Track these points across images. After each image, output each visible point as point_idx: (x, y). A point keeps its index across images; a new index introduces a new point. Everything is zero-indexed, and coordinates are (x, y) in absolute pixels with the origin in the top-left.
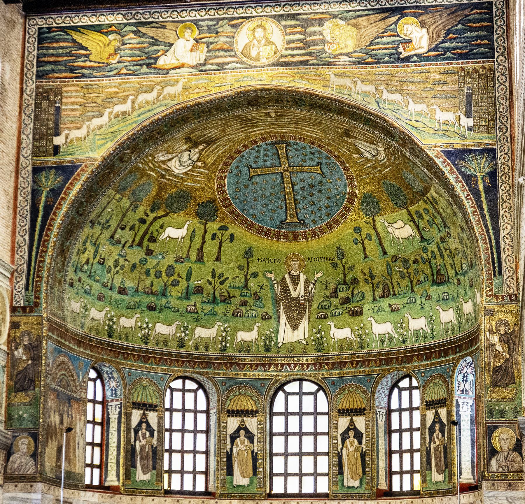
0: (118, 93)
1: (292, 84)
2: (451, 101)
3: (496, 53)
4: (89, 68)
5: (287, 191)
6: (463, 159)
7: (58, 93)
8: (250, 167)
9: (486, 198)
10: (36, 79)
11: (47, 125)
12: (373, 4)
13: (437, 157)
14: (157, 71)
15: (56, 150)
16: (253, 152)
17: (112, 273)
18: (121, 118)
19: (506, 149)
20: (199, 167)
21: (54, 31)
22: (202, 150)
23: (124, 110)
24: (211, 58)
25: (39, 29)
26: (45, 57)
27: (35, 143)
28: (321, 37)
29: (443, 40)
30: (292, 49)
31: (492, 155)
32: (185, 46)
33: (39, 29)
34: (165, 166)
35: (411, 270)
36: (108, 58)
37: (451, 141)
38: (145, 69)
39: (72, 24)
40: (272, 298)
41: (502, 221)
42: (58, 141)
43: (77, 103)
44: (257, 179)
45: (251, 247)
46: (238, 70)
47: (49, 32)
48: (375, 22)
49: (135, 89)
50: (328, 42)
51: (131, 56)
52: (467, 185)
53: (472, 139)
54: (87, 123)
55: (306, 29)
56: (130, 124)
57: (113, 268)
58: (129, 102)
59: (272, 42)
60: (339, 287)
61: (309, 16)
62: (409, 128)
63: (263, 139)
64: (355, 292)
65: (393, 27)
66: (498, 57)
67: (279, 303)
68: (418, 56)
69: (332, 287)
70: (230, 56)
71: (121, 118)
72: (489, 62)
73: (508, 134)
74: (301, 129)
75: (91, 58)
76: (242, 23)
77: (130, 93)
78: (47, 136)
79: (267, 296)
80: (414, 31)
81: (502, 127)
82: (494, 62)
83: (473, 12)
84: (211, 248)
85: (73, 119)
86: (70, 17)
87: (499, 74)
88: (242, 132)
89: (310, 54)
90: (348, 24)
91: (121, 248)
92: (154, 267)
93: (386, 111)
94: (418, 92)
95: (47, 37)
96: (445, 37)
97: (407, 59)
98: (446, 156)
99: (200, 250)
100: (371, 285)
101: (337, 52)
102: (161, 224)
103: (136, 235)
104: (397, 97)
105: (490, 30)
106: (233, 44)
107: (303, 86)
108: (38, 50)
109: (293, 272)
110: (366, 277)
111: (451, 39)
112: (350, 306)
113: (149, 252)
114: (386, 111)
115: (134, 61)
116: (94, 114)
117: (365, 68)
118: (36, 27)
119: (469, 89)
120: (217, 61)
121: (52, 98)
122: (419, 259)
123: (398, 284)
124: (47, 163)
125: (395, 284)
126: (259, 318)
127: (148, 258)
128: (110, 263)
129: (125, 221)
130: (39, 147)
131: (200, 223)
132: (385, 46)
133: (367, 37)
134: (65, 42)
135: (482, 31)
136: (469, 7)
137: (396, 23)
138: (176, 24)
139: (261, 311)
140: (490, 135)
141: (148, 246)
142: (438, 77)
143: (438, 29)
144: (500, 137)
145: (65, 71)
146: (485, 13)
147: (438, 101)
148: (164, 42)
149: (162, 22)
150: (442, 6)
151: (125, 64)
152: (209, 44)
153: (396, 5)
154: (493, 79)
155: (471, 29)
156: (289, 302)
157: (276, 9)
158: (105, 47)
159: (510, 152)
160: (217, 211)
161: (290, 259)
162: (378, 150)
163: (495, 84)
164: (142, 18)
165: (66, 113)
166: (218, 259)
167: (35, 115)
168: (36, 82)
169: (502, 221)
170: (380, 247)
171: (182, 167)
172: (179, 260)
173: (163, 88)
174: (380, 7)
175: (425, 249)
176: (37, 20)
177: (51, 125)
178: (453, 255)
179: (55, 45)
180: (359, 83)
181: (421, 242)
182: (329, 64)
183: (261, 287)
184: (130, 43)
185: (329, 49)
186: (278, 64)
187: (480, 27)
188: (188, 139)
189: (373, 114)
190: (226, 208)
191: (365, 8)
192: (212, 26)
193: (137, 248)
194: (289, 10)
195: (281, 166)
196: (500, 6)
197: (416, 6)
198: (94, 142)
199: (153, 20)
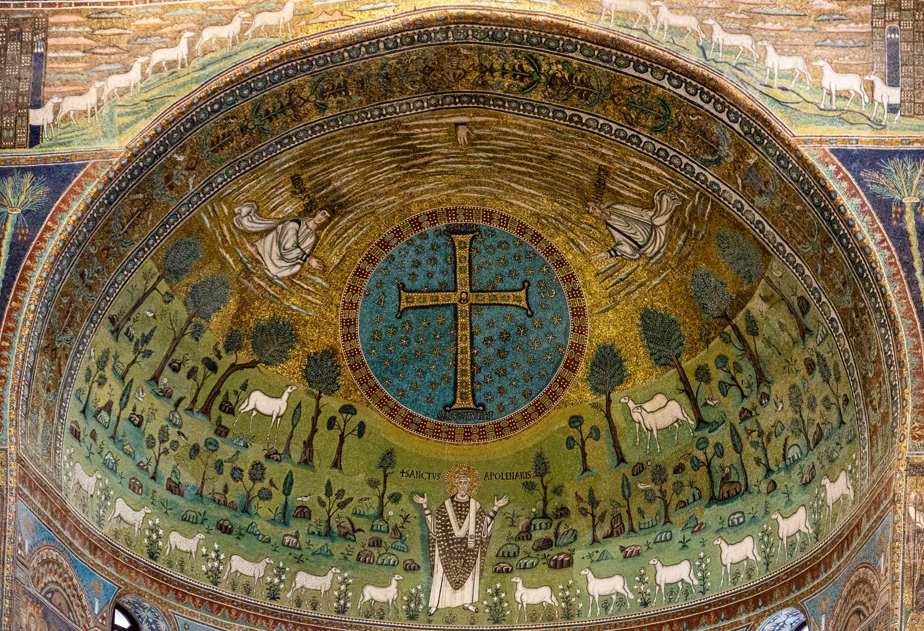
5: (461, 345)
8: (402, 287)
22: (321, 227)
23: (175, 58)
35: (668, 486)
40: (422, 537)
44: (411, 316)
45: (392, 450)
60: (534, 522)
62: (766, 103)
63: (433, 217)
64: (562, 530)
67: (434, 547)
69: (522, 522)
71: (166, 73)
79: (413, 533)
100: (590, 517)
110: (582, 505)
112: (553, 553)
123: (641, 512)
125: (634, 512)
126: (400, 567)
139: (403, 557)
156: (449, 545)
160: (339, 374)
162: (653, 227)
181: (698, 429)
183: (405, 519)
190: (353, 369)
195: (455, 290)
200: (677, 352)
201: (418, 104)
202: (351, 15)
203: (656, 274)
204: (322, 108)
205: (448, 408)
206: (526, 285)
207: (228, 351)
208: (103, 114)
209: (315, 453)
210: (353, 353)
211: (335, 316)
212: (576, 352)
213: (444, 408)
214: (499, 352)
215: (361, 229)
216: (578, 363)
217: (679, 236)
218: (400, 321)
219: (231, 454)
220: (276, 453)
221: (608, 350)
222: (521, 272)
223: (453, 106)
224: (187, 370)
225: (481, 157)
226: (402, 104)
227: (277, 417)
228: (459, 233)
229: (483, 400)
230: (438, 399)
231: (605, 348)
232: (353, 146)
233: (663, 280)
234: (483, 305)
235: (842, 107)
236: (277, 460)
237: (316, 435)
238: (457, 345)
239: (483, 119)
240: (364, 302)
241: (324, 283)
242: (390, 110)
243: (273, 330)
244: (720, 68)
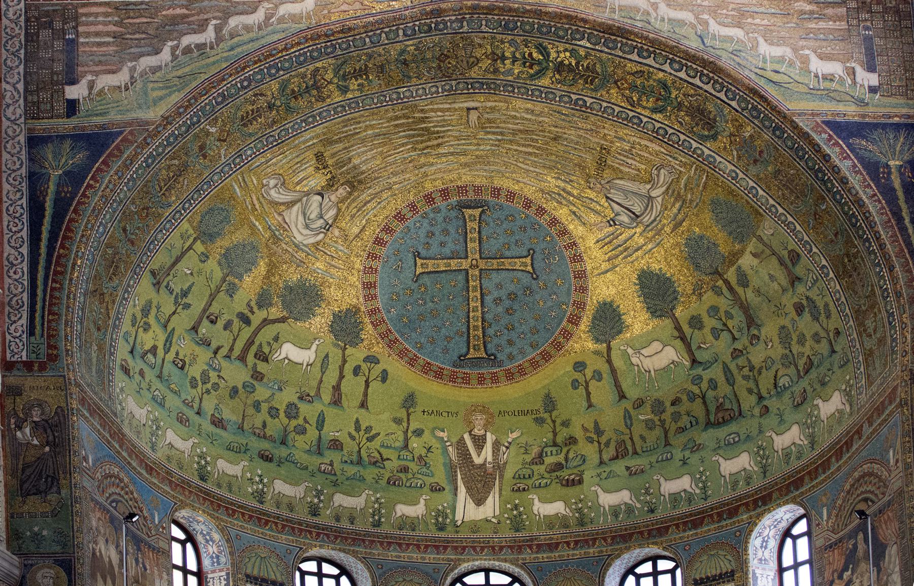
18: (196, 54)
27: (30, 98)
37: (841, 108)
42: (73, 92)
102: (275, 334)
109: (476, 430)
201: (434, 89)
204: (344, 90)
206: (531, 253)
207: (260, 307)
219: (267, 396)
220: (308, 395)
222: (527, 242)
223: (465, 91)
224: (224, 322)
225: (490, 139)
226: (419, 89)
228: (469, 207)
235: (828, 87)
236: (309, 401)
237: (344, 380)
239: (493, 104)
242: (407, 94)
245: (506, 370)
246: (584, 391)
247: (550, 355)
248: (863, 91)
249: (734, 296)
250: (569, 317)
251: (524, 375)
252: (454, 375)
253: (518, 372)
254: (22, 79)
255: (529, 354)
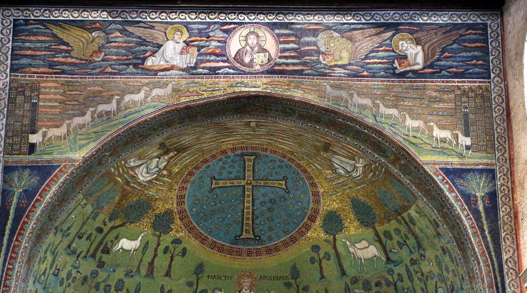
0: (101, 92)
1: (289, 93)
2: (448, 119)
3: (492, 74)
4: (71, 64)
5: (246, 205)
6: (462, 178)
7: (35, 88)
9: (486, 219)
10: (10, 73)
11: (22, 122)
12: (368, 18)
13: (435, 174)
14: (144, 72)
15: (32, 148)
16: (220, 163)
17: (64, 286)
18: (105, 118)
19: (506, 170)
20: (164, 176)
21: (31, 24)
22: (171, 158)
23: (109, 109)
24: (202, 61)
25: (14, 20)
26: (21, 50)
27: (8, 141)
28: (315, 48)
29: (438, 58)
30: (286, 57)
31: (491, 175)
32: (174, 48)
33: (14, 20)
34: (132, 173)
36: (91, 56)
37: (450, 159)
38: (131, 69)
39: (52, 18)
41: (503, 243)
42: (34, 139)
43: (56, 100)
44: (218, 191)
46: (231, 76)
47: (26, 25)
48: (370, 36)
49: (121, 88)
50: (323, 53)
51: (117, 54)
52: (467, 205)
53: (470, 158)
54: (67, 122)
55: (300, 39)
56: (115, 125)
57: (65, 280)
58: (114, 101)
59: (266, 50)
61: (303, 26)
63: (233, 150)
65: (388, 42)
66: (494, 78)
68: (414, 72)
70: (222, 61)
71: (105, 118)
72: (485, 82)
73: (506, 155)
74: (276, 141)
75: (73, 54)
76: (234, 28)
77: (115, 92)
78: (22, 133)
80: (409, 47)
81: (500, 147)
82: (489, 82)
83: (467, 33)
84: (162, 262)
85: (52, 117)
86: (49, 11)
87: (495, 95)
88: (214, 141)
89: (304, 64)
90: (343, 37)
91: (74, 258)
92: (104, 281)
93: (384, 125)
94: (414, 108)
95: (23, 29)
96: (440, 55)
97: (403, 75)
98: (444, 174)
99: (151, 264)
101: (332, 64)
103: (91, 245)
104: (394, 112)
105: (485, 51)
106: (225, 50)
107: (299, 95)
108: (13, 42)
111: (446, 57)
113: (101, 264)
114: (384, 125)
115: (120, 60)
116: (75, 112)
117: (361, 81)
118: (12, 18)
119: (466, 108)
120: (208, 65)
121: (28, 93)
122: (383, 282)
124: (21, 161)
127: (99, 270)
128: (63, 274)
129: (82, 231)
130: (11, 145)
131: (154, 235)
132: (381, 61)
133: (362, 51)
134: (44, 36)
135: (477, 51)
136: (464, 27)
137: (391, 38)
138: (165, 25)
140: (488, 155)
141: (101, 257)
142: (434, 94)
143: (432, 47)
144: (498, 158)
145: (44, 66)
146: (480, 34)
147: (435, 118)
148: (152, 42)
149: (150, 22)
150: (437, 24)
151: (110, 63)
152: (200, 48)
153: (390, 21)
154: (490, 99)
155: (467, 49)
157: (269, 17)
158: (88, 44)
159: (509, 173)
160: (173, 223)
161: (240, 277)
162: (355, 167)
163: (491, 104)
164: (128, 17)
165: (44, 110)
166: (168, 274)
167: (8, 111)
168: (11, 76)
169: (503, 243)
170: (338, 267)
171: (148, 175)
172: (128, 274)
173: (151, 89)
174: (374, 21)
175: (391, 272)
176: (13, 11)
177: (26, 121)
178: (425, 278)
179: (33, 38)
180: (355, 95)
182: (325, 75)
184: (115, 42)
185: (324, 60)
186: (271, 72)
187: (475, 47)
188: (162, 145)
189: (371, 128)
191: (360, 22)
192: (203, 29)
193: (90, 259)
194: (281, 18)
195: (244, 179)
196: (494, 28)
197: (411, 23)
198: (75, 142)
199: (140, 19)
200: (372, 221)
202: (202, 93)
203: (358, 185)
205: (237, 238)
207: (110, 220)
208: (71, 138)
209: (155, 269)
210: (180, 212)
211: (174, 195)
212: (315, 212)
213: (235, 238)
214: (269, 209)
215: (193, 156)
216: (316, 218)
217: (370, 173)
218: (211, 194)
221: (333, 214)
227: (134, 251)
229: (259, 234)
230: (232, 233)
231: (332, 212)
232: (195, 130)
233: (362, 188)
234: (260, 186)
237: (156, 258)
238: (244, 205)
240: (190, 187)
241: (169, 180)
243: (137, 206)
244: (384, 126)
245: (266, 247)
246: (318, 265)
247: (296, 239)
248: (462, 149)
249: (408, 227)
250: (309, 216)
251: (279, 251)
252: (231, 250)
253: (275, 249)
254: (4, 128)
255: (282, 237)
